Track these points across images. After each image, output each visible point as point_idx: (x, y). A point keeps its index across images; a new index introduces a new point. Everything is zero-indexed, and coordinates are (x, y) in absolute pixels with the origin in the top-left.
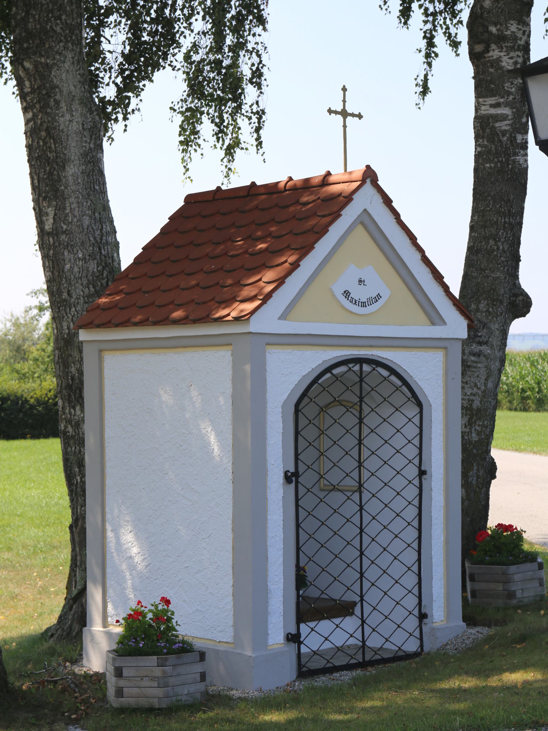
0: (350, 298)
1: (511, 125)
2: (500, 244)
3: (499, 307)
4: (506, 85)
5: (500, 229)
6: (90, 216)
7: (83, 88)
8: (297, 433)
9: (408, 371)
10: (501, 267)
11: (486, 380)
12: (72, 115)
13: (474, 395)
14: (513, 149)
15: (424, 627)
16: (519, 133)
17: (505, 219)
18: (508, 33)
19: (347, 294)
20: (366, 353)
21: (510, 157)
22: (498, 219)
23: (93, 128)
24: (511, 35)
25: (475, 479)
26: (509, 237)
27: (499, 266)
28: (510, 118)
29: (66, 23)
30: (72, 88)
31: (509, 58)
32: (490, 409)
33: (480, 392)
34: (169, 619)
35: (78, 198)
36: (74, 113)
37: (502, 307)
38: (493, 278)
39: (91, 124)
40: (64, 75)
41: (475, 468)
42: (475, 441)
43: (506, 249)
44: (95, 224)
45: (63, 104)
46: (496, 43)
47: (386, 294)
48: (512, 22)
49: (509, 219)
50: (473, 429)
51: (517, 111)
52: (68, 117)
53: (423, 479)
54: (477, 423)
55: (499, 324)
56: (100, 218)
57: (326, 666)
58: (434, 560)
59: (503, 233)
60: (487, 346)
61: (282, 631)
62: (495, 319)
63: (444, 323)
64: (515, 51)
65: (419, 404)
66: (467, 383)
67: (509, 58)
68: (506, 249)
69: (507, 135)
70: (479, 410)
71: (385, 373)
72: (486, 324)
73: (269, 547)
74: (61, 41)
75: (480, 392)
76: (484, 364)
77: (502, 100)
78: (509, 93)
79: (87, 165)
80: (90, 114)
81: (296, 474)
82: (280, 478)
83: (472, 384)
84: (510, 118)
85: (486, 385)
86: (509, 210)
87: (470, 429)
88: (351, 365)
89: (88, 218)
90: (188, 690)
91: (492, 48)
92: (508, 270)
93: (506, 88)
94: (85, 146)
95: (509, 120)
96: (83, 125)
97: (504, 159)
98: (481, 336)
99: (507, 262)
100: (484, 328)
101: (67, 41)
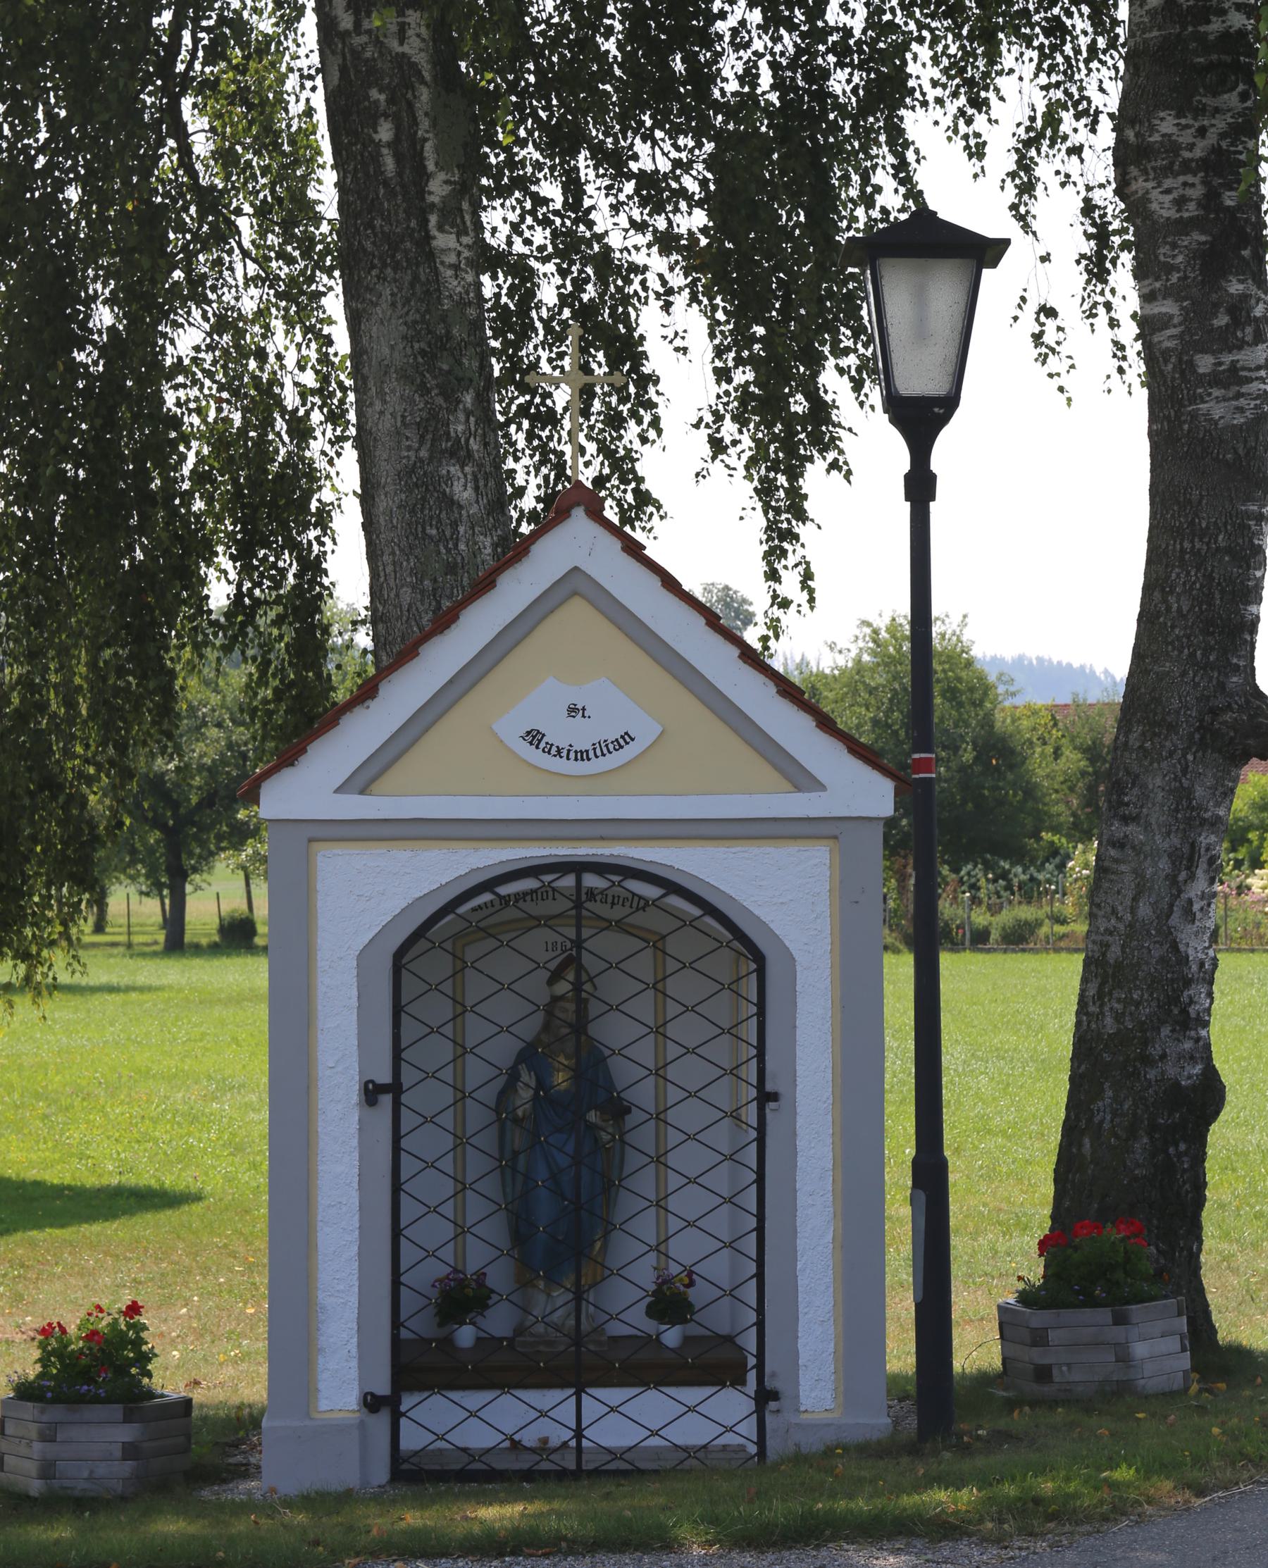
0: (542, 745)
1: (1180, 336)
2: (1172, 599)
3: (1166, 739)
4: (1162, 251)
5: (1173, 567)
6: (413, 588)
7: (409, 351)
8: (398, 1010)
9: (722, 888)
10: (1174, 649)
11: (1134, 899)
12: (384, 402)
13: (1111, 934)
14: (1189, 390)
15: (769, 1418)
16: (1204, 351)
17: (1181, 544)
18: (1156, 138)
19: (534, 737)
20: (591, 852)
21: (1185, 406)
22: (1167, 545)
23: (427, 420)
24: (1161, 143)
25: (1108, 1117)
26: (1194, 583)
27: (1170, 648)
28: (1176, 321)
29: (383, 232)
30: (387, 351)
31: (1162, 193)
32: (1147, 963)
33: (1121, 927)
34: (139, 1342)
35: (393, 553)
36: (388, 398)
37: (1175, 738)
38: (1157, 673)
39: (424, 415)
40: (375, 329)
41: (1109, 1093)
42: (1109, 1035)
43: (1185, 609)
44: (422, 601)
45: (371, 384)
46: (1137, 163)
47: (646, 731)
48: (1162, 114)
49: (1192, 542)
50: (1106, 1008)
51: (1193, 304)
52: (378, 406)
53: (767, 1111)
54: (1116, 995)
55: (1165, 776)
56: (434, 589)
57: (469, 1467)
58: (802, 1282)
59: (1178, 575)
60: (1138, 824)
61: (356, 1385)
62: (1155, 765)
63: (818, 786)
64: (1176, 175)
65: (759, 958)
66: (1098, 906)
67: (1162, 193)
68: (1185, 609)
69: (1173, 360)
70: (1118, 966)
71: (651, 891)
72: (1137, 776)
73: (320, 1224)
74: (373, 267)
75: (1121, 927)
76: (1133, 864)
77: (1158, 285)
78: (1170, 269)
79: (411, 493)
80: (422, 396)
81: (395, 1088)
82: (353, 1093)
83: (1109, 909)
84: (1176, 321)
85: (1133, 910)
86: (1192, 523)
87: (1101, 1006)
88: (547, 878)
89: (410, 590)
90: (92, 1472)
91: (1132, 175)
92: (1192, 655)
93: (1162, 258)
94: (408, 457)
95: (1175, 327)
96: (403, 417)
97: (1173, 413)
98: (1127, 804)
99: (1188, 638)
100: (1133, 784)
101: (385, 265)
